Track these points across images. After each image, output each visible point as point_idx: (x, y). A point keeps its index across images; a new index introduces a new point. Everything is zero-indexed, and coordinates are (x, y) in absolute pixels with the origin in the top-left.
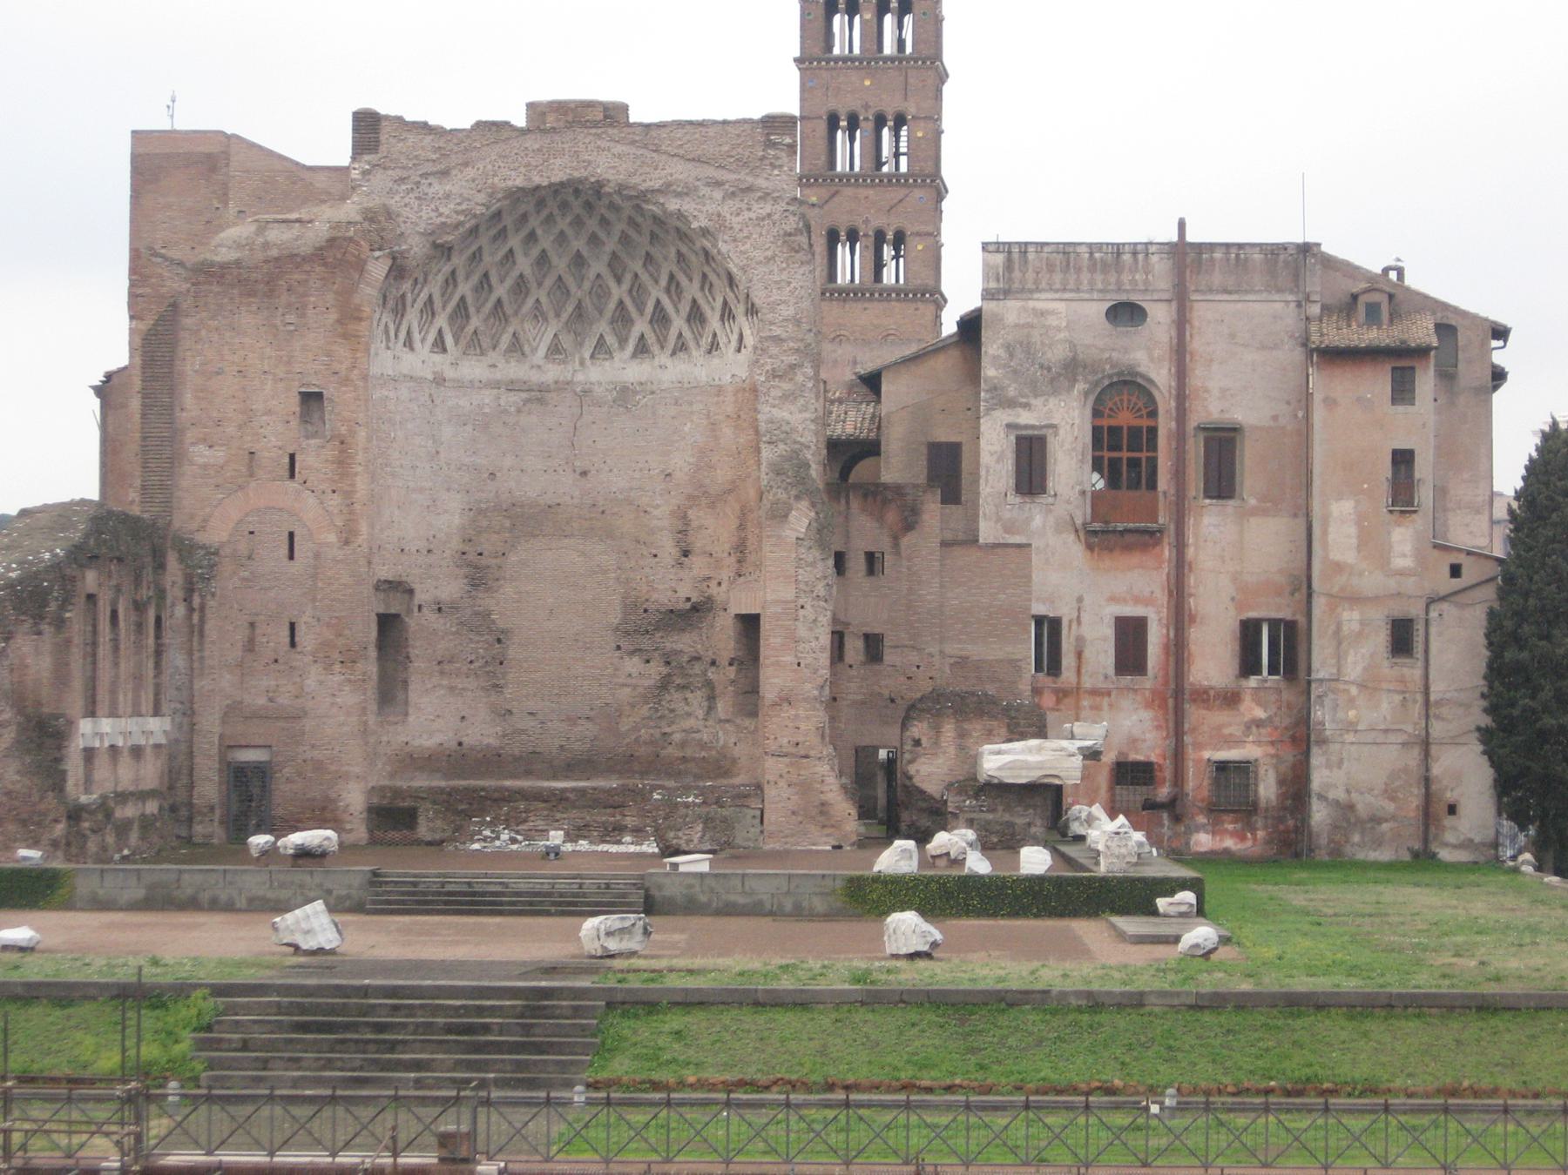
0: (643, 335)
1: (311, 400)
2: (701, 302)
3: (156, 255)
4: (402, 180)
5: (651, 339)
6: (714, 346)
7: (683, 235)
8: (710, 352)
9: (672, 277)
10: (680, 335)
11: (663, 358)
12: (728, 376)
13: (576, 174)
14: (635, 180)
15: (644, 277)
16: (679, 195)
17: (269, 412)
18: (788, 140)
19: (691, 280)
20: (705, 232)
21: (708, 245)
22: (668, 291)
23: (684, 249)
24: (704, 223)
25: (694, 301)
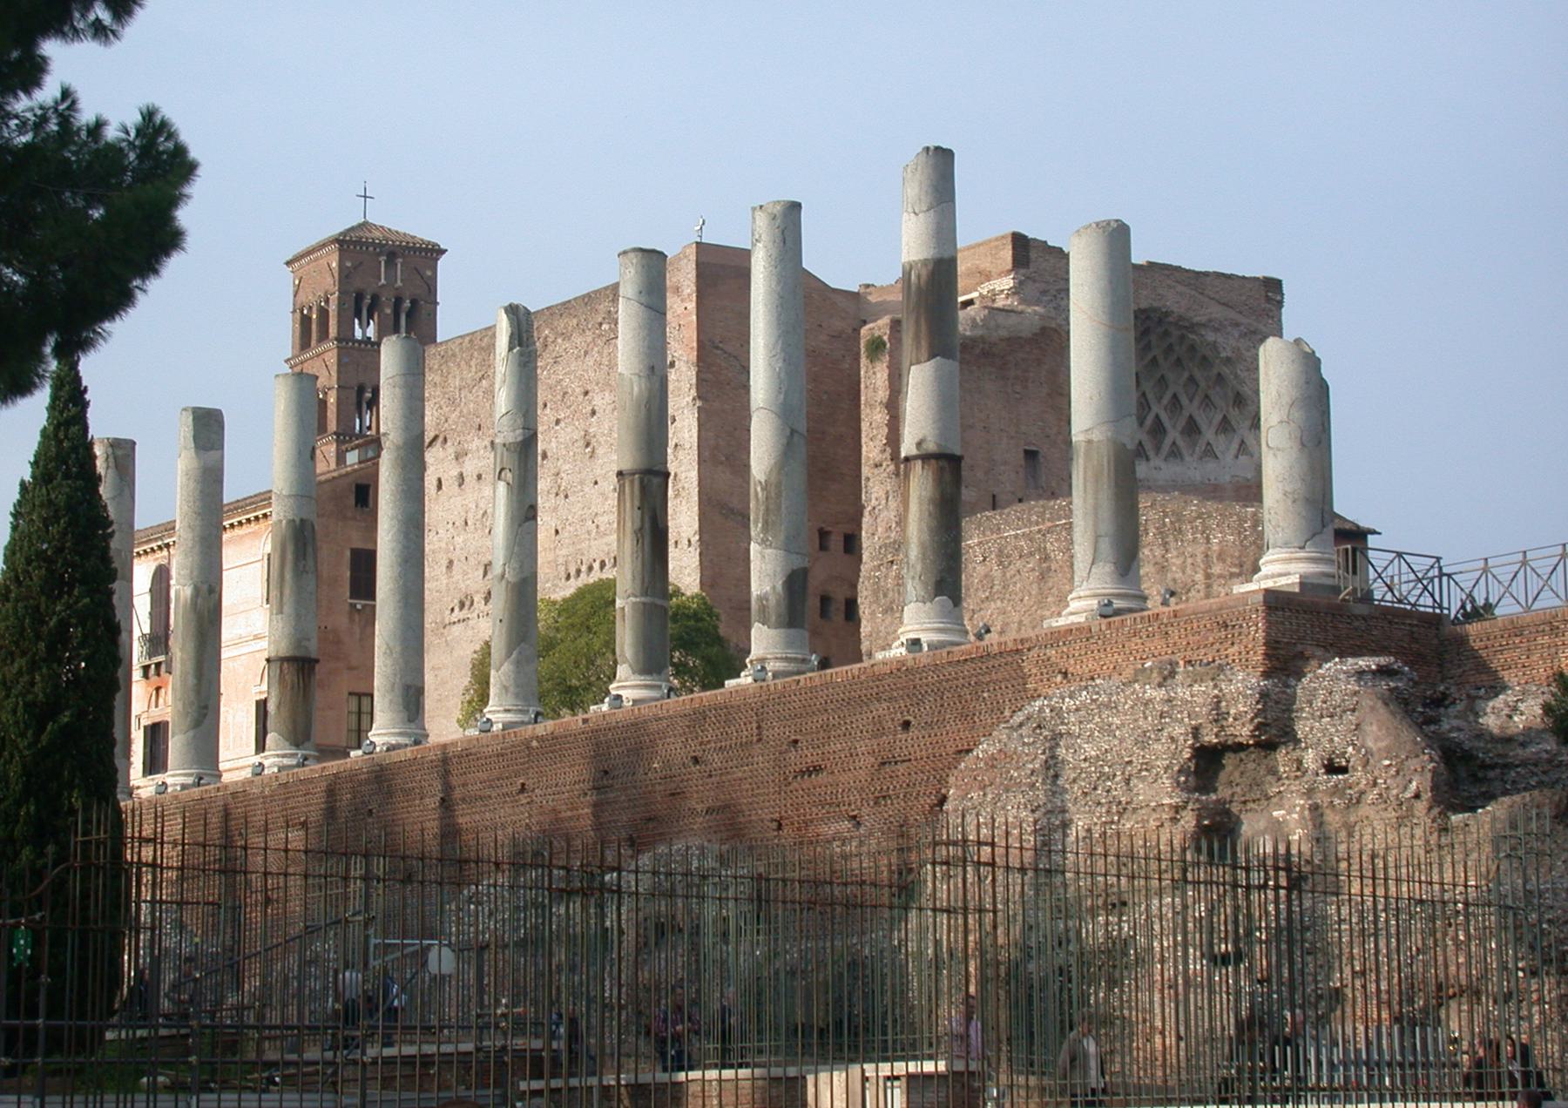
0: (1140, 443)
1: (1031, 455)
2: (1198, 419)
3: (717, 348)
4: (1044, 292)
5: (1148, 446)
6: (1209, 452)
7: (1205, 362)
8: (1201, 458)
9: (1175, 396)
10: (1174, 443)
11: (1156, 461)
12: (1228, 478)
13: (1155, 304)
14: (1191, 314)
15: (1150, 396)
16: (1216, 330)
17: (1005, 463)
18: (1279, 298)
19: (1191, 401)
20: (1228, 359)
21: (1226, 371)
22: (1165, 409)
23: (1198, 374)
24: (1229, 354)
25: (1191, 417)
